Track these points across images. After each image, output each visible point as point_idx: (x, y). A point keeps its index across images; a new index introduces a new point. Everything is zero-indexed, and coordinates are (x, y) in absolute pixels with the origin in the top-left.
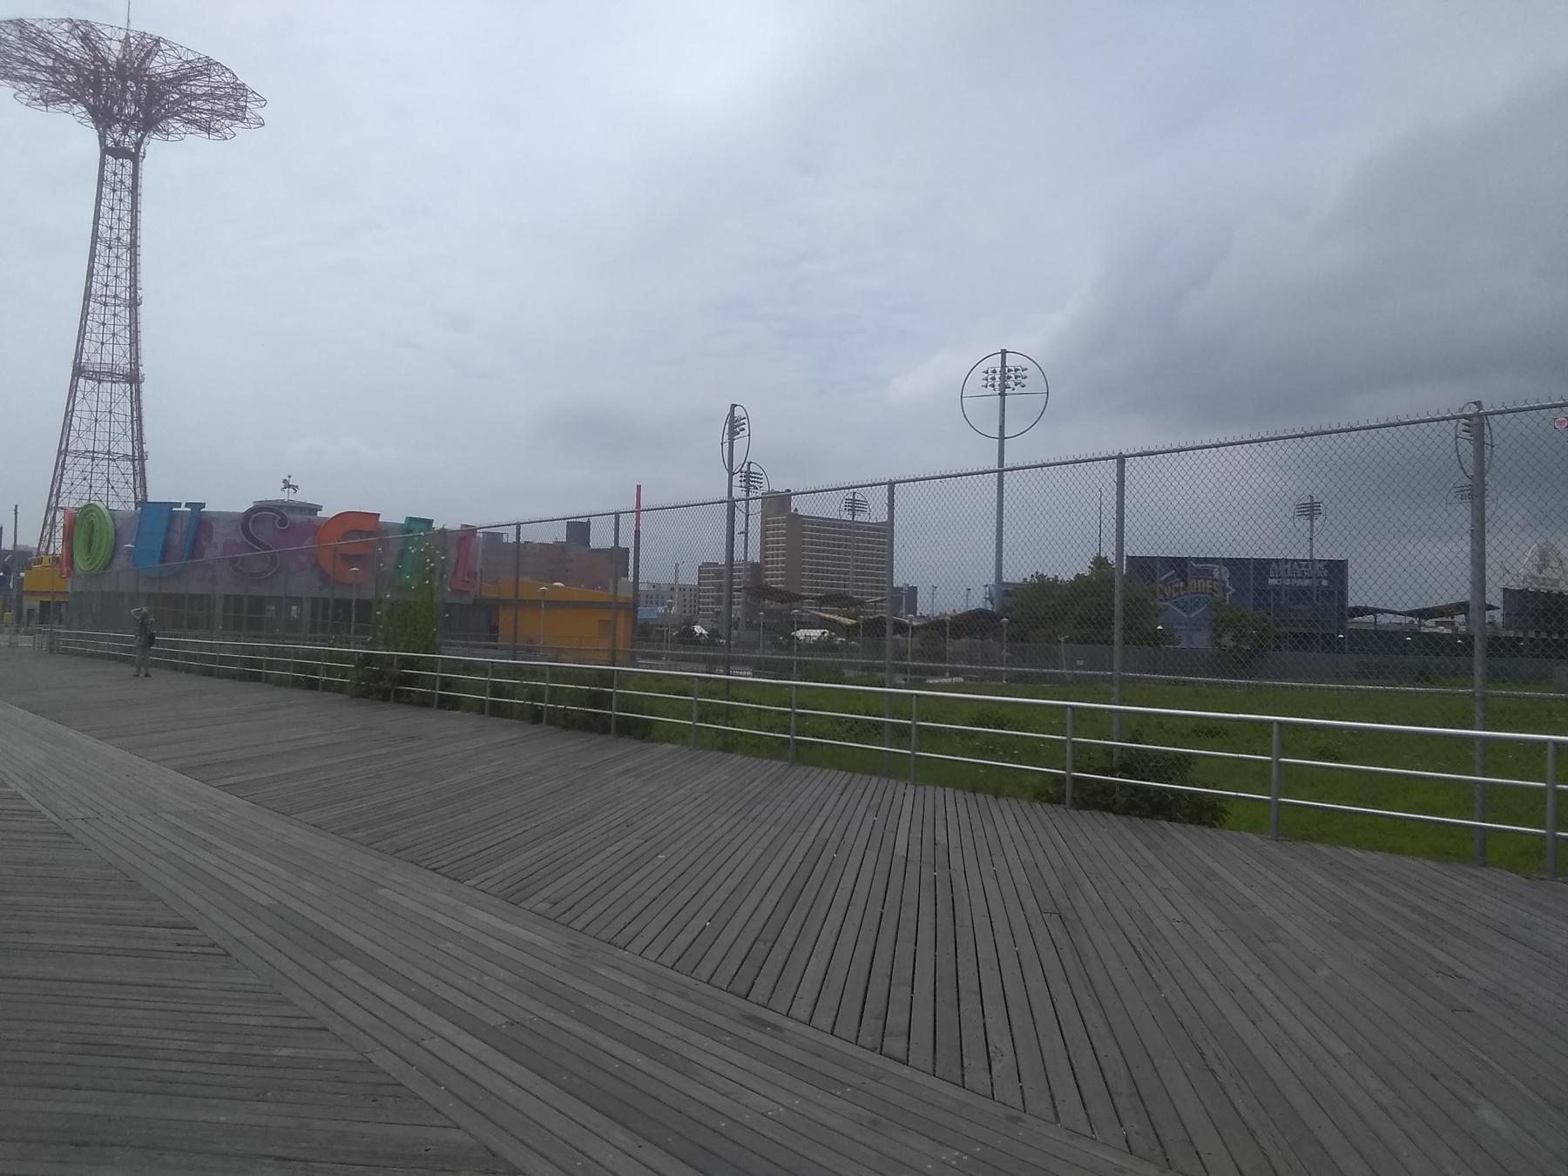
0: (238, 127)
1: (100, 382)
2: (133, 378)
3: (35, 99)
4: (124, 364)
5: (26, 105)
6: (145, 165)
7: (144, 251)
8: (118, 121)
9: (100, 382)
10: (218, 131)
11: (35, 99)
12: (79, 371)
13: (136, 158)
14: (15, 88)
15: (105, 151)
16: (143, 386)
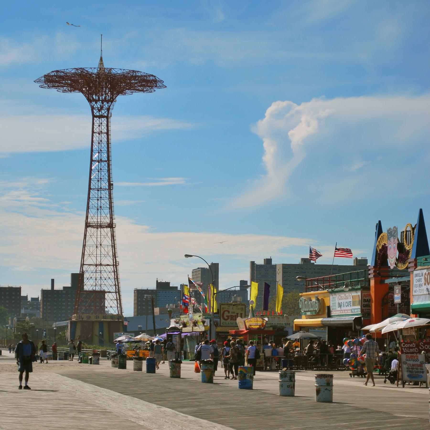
0: (155, 89)
1: (97, 228)
2: (111, 226)
3: (64, 90)
4: (108, 221)
5: (62, 92)
6: (112, 120)
7: (113, 163)
8: (99, 100)
9: (97, 228)
10: (147, 90)
11: (66, 90)
12: (87, 225)
13: (107, 117)
14: (57, 89)
15: (94, 116)
16: (116, 230)
